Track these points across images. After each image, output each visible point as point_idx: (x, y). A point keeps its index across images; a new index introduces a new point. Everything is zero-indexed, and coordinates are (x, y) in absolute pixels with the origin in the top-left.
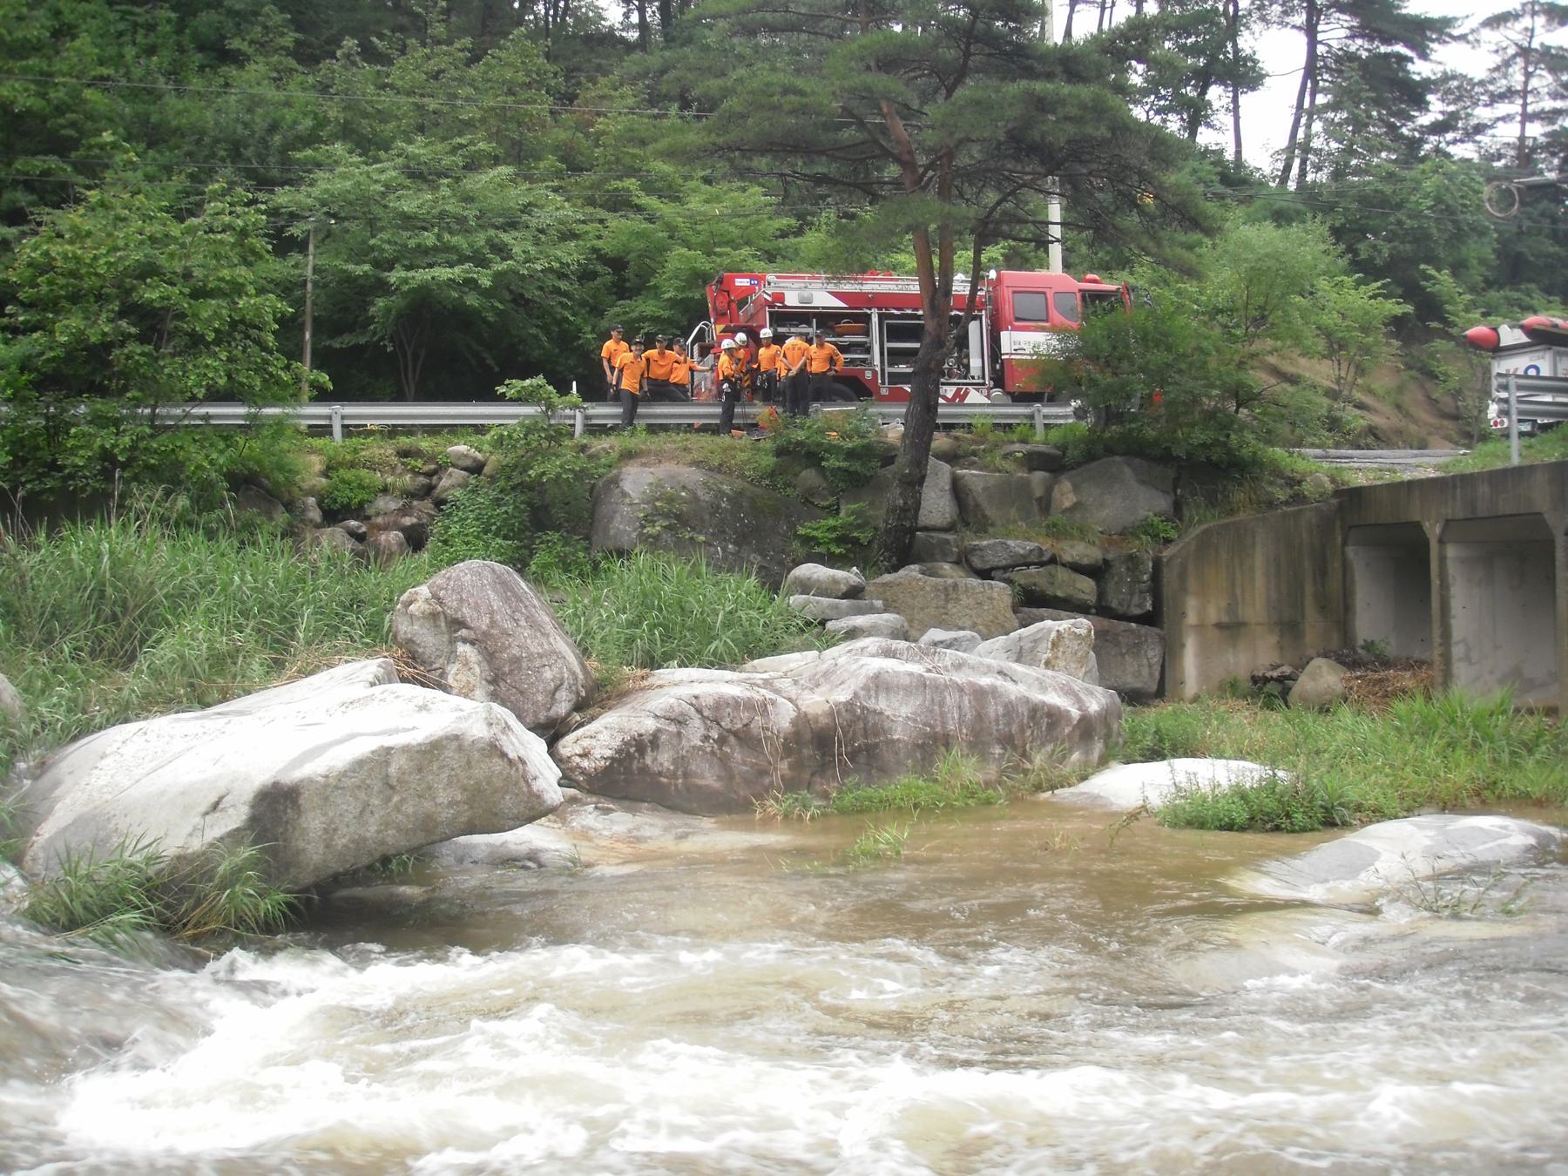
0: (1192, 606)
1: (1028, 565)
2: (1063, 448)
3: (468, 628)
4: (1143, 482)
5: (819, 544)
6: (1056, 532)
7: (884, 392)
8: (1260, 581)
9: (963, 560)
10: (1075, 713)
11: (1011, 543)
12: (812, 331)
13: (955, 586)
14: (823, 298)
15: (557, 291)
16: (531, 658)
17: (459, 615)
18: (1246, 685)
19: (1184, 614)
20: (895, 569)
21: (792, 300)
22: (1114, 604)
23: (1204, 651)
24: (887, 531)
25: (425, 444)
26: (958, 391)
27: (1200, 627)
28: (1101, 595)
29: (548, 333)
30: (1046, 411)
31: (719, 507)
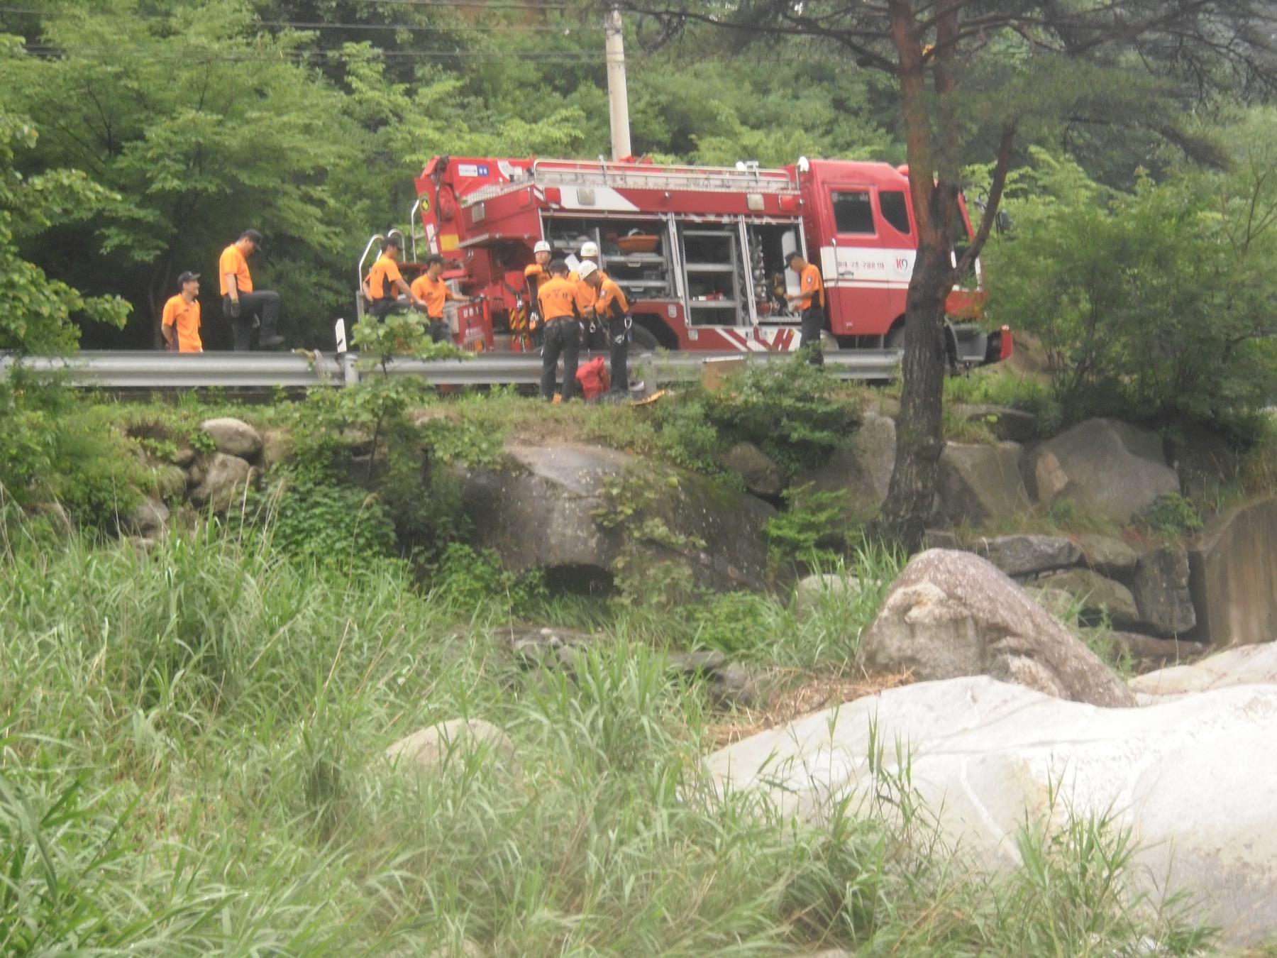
1: (1054, 568)
3: (1014, 635)
4: (1133, 452)
11: (1034, 539)
14: (609, 201)
17: (998, 619)
21: (570, 200)
22: (1155, 619)
25: (171, 418)
26: (780, 333)
31: (679, 500)
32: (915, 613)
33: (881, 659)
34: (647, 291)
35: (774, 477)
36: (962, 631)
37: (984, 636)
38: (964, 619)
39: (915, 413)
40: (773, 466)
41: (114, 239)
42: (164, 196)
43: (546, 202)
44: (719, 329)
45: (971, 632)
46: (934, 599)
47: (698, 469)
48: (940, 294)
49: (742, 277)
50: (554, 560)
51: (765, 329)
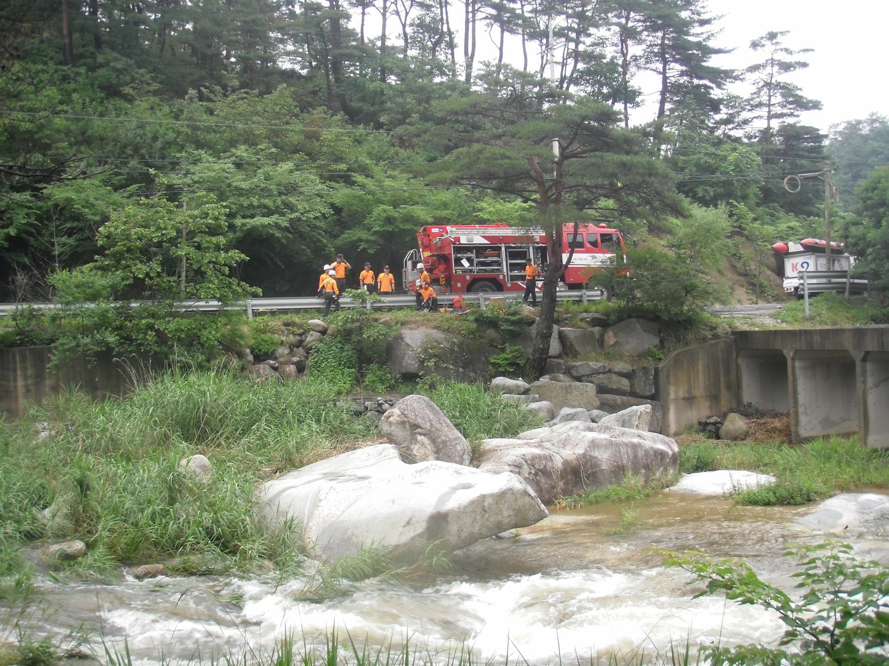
0: (672, 390)
1: (598, 374)
2: (607, 314)
4: (645, 331)
5: (500, 366)
6: (609, 357)
7: (509, 285)
8: (701, 377)
9: (568, 372)
10: (670, 453)
11: (590, 363)
12: (473, 255)
13: (570, 386)
14: (479, 240)
15: (316, 227)
16: (450, 440)
18: (696, 426)
19: (669, 394)
20: (537, 379)
21: (464, 240)
22: (638, 391)
23: (678, 412)
24: (534, 360)
25: (297, 319)
27: (676, 399)
28: (632, 386)
29: (308, 247)
30: (588, 293)
34: (493, 270)
41: (363, 246)
42: (376, 233)
50: (404, 371)
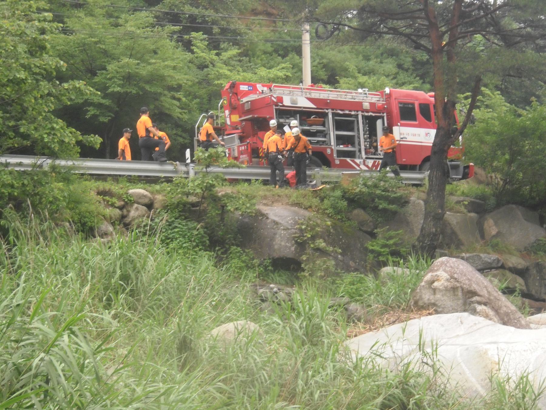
1: (491, 268)
3: (479, 296)
4: (525, 220)
11: (482, 255)
14: (304, 103)
17: (472, 289)
21: (287, 102)
22: (533, 292)
25: (115, 188)
26: (375, 162)
31: (330, 232)
32: (436, 284)
33: (420, 303)
34: (318, 142)
35: (371, 224)
36: (456, 293)
37: (466, 296)
38: (457, 288)
39: (433, 199)
40: (371, 219)
41: (92, 111)
42: (113, 94)
43: (277, 103)
44: (348, 160)
45: (460, 293)
46: (445, 278)
47: (339, 219)
48: (446, 148)
49: (359, 138)
50: (276, 255)
51: (368, 160)
